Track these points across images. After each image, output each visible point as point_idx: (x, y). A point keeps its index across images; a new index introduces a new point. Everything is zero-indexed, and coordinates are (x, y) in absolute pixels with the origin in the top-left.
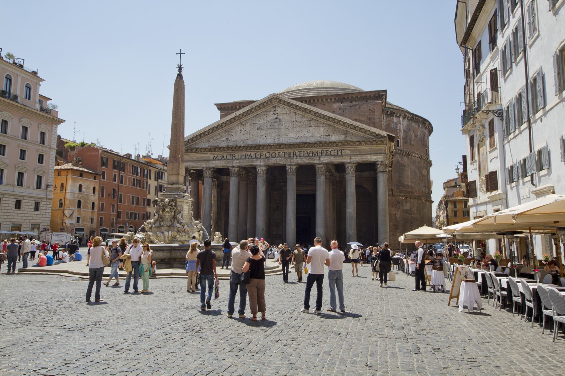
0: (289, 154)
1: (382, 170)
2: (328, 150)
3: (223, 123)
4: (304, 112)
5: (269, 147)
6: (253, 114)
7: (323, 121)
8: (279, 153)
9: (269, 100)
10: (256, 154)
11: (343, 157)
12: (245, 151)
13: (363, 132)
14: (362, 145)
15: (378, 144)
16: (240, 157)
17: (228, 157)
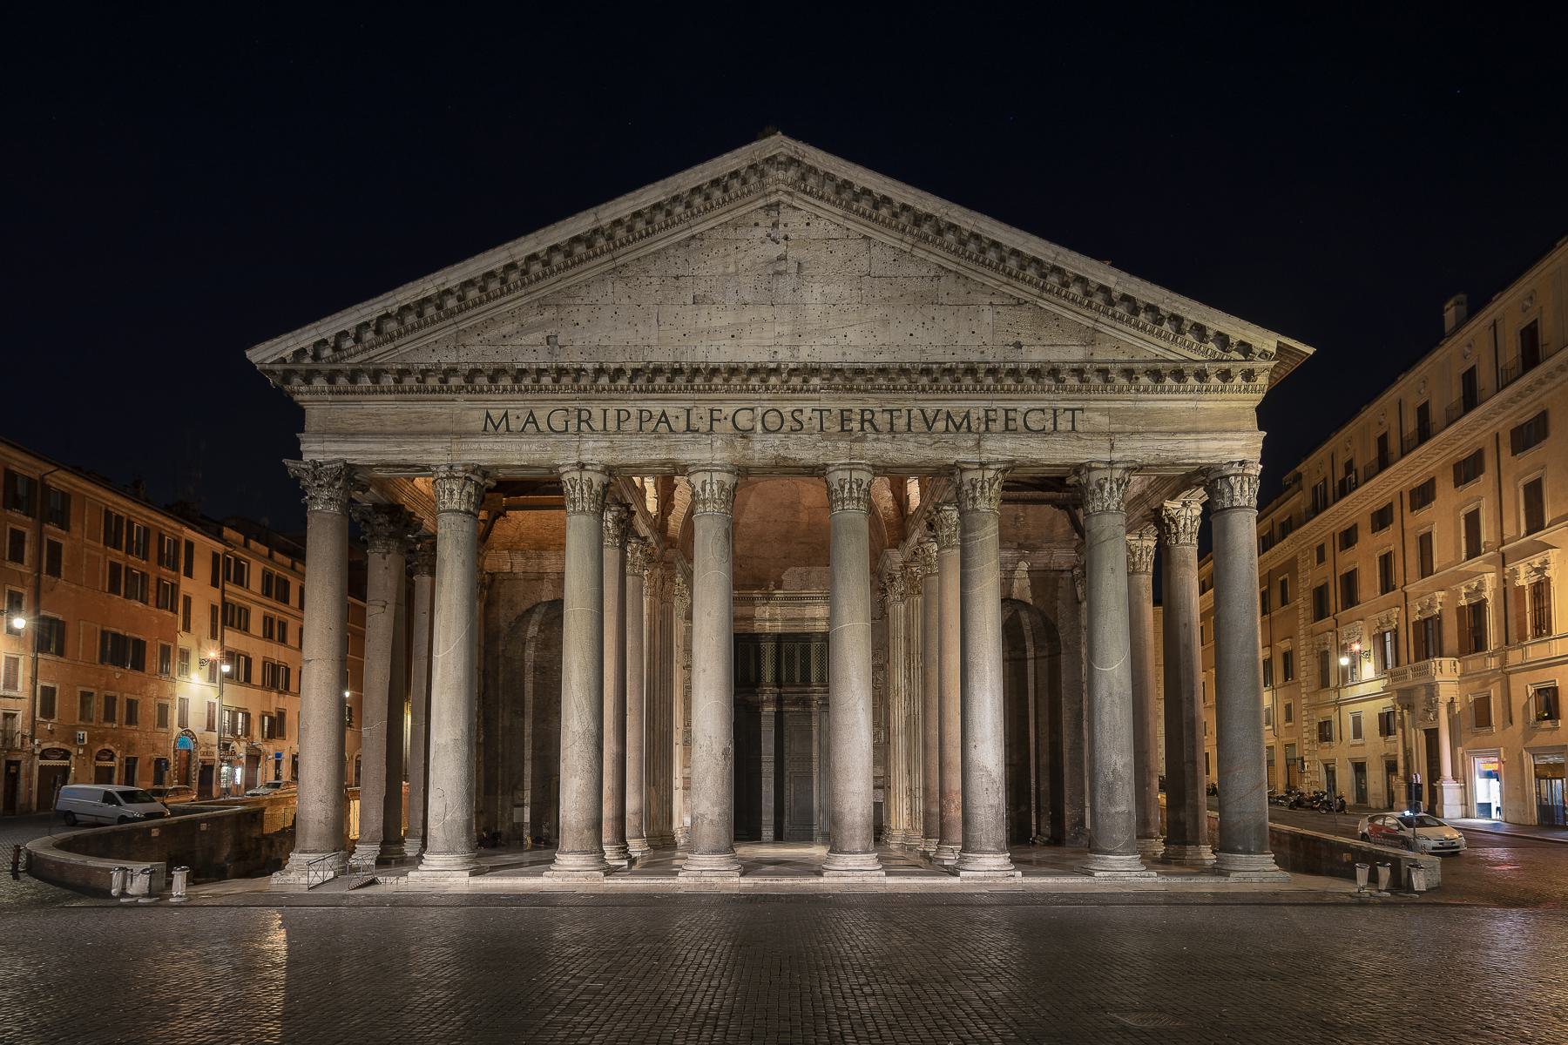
0: (844, 417)
1: (1244, 502)
2: (1015, 410)
3: (533, 257)
4: (911, 233)
5: (754, 381)
6: (676, 229)
7: (992, 280)
8: (796, 414)
9: (751, 167)
10: (688, 411)
11: (1079, 439)
12: (636, 395)
13: (1166, 338)
14: (1162, 391)
15: (1231, 391)
16: (611, 425)
17: (558, 424)
